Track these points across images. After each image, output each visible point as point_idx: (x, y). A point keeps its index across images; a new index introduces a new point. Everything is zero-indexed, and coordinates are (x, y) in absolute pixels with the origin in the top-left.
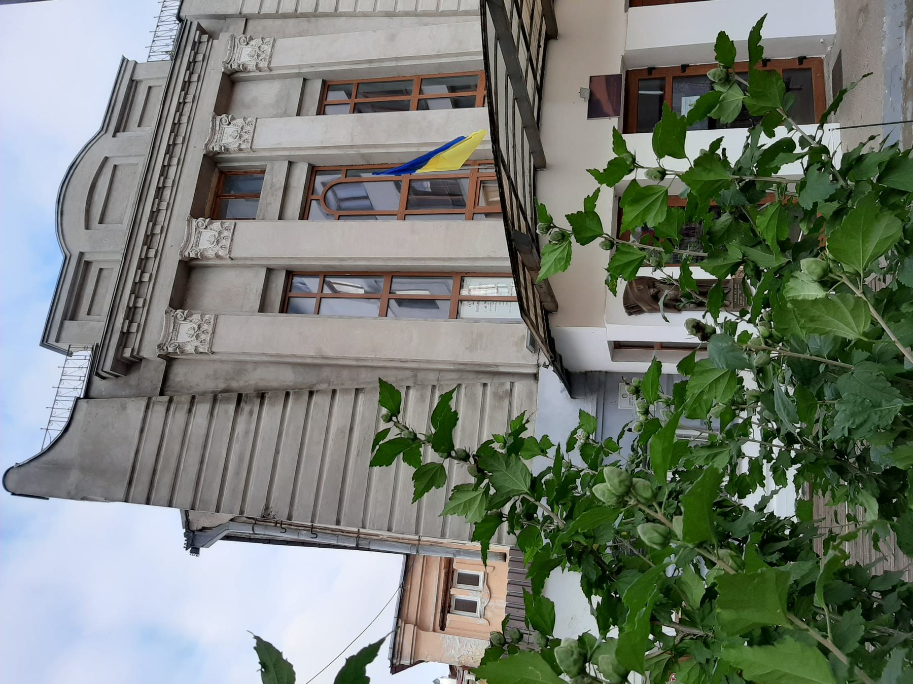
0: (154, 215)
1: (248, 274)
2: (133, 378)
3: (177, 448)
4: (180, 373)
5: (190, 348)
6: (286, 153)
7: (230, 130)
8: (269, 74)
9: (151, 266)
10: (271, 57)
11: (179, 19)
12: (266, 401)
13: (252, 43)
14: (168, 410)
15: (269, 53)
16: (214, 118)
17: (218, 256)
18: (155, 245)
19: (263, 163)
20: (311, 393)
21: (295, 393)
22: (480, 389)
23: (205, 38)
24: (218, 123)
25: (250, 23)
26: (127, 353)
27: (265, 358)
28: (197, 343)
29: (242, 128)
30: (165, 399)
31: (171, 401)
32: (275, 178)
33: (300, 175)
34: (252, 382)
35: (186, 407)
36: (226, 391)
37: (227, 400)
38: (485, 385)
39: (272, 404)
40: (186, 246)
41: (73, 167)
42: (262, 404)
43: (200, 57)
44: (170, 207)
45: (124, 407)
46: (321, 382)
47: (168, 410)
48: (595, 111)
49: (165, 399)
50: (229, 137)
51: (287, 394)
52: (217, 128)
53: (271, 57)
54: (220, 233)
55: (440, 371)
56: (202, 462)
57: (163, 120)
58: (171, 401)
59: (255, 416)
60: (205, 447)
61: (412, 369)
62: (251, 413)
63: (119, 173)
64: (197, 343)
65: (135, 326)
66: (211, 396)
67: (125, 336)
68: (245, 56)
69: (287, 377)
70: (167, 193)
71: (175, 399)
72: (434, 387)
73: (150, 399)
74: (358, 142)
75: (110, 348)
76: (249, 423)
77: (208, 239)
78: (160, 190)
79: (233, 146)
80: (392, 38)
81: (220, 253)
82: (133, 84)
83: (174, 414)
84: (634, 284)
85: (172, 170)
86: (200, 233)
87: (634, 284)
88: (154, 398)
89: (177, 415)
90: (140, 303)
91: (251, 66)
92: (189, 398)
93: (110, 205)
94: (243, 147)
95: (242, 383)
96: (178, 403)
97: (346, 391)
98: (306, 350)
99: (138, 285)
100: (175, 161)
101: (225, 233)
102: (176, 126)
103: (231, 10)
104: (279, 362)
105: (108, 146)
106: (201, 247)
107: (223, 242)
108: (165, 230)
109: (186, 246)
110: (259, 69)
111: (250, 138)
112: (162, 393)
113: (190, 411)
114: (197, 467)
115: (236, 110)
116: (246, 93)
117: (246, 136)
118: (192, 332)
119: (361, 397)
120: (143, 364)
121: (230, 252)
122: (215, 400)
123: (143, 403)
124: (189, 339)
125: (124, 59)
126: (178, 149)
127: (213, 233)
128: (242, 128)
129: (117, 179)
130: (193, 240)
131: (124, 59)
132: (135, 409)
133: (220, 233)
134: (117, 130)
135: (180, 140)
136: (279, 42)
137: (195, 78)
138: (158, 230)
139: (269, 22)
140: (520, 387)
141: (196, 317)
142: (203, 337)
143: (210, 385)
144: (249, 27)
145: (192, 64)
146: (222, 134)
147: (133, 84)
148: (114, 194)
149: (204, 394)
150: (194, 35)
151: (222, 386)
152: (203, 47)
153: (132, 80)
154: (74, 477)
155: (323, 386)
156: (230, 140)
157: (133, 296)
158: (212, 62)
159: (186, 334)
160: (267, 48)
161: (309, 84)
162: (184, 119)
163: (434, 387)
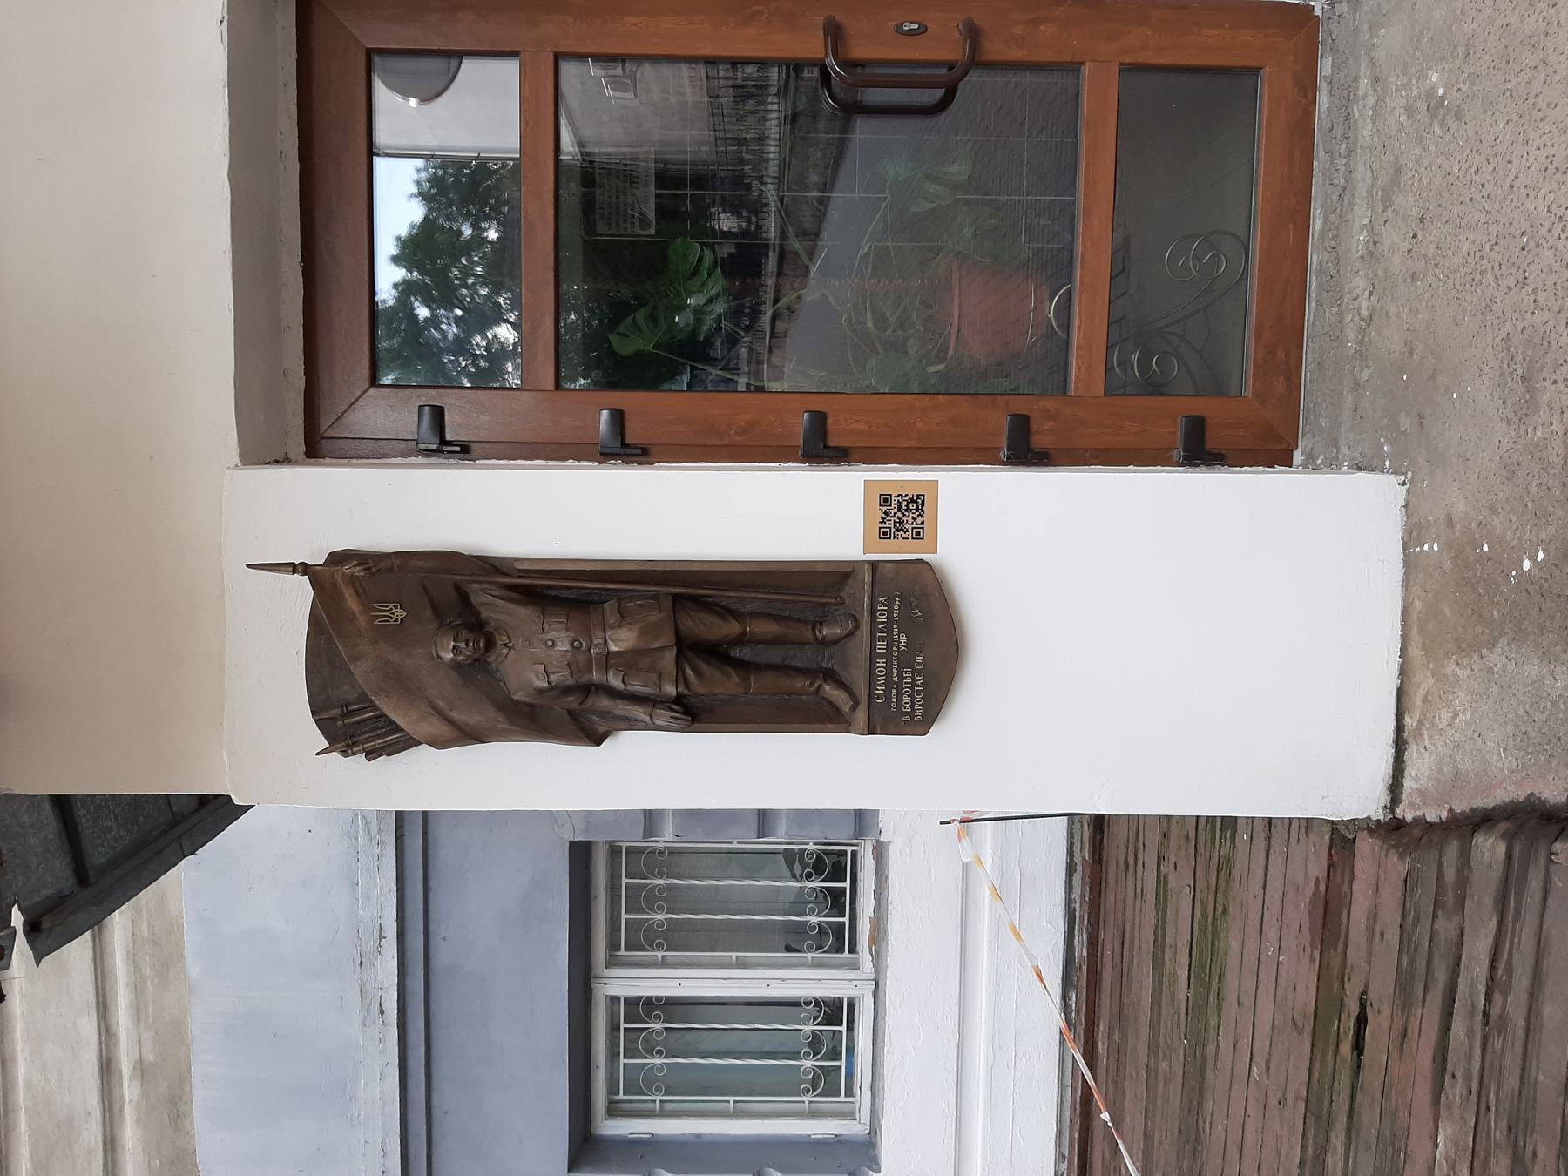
84: (352, 603)
87: (352, 603)
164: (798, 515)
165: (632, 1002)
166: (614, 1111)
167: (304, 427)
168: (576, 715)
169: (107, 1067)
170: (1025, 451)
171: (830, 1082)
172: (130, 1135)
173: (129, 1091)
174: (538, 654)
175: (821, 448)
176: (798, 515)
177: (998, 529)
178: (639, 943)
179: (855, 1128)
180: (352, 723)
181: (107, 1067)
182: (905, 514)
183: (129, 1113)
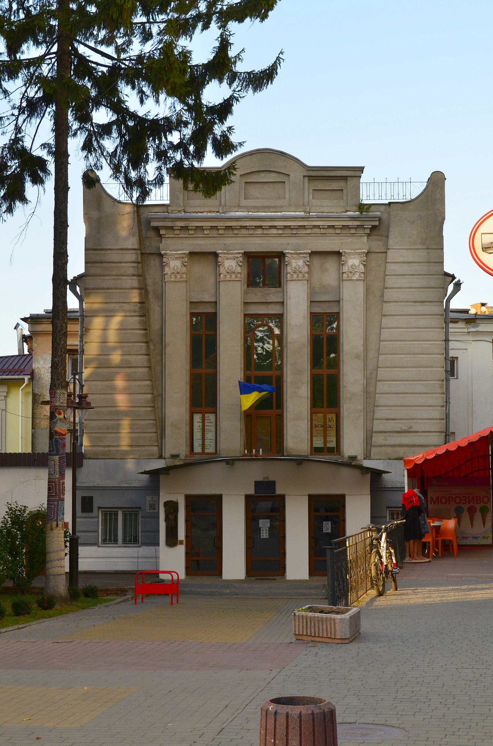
0: (245, 227)
1: (213, 291)
2: (151, 234)
3: (114, 273)
4: (154, 262)
5: (167, 269)
6: (285, 302)
7: (301, 263)
8: (341, 279)
9: (215, 232)
10: (350, 280)
11: (390, 203)
12: (141, 318)
13: (362, 266)
14: (134, 262)
15: (353, 278)
16: (307, 253)
17: (220, 274)
18: (227, 232)
19: (282, 285)
20: (147, 342)
21: (146, 333)
22: (154, 430)
23: (368, 231)
24: (305, 255)
25: (384, 255)
26: (162, 232)
27: (164, 313)
28: (169, 273)
29: (300, 272)
30: (140, 260)
31: (138, 263)
32: (273, 295)
33: (274, 310)
34: (152, 306)
35: (136, 273)
36: (147, 291)
37: (140, 295)
38: (156, 433)
39: (140, 322)
40: (225, 253)
41: (282, 154)
42: (140, 316)
43: (353, 231)
44: (251, 236)
45: (133, 235)
46: (154, 345)
47: (134, 262)
48: (257, 484)
49: (140, 260)
50: (295, 264)
51: (146, 329)
52: (301, 255)
53: (350, 280)
54: (232, 273)
55: (162, 408)
56: (108, 289)
57: (306, 219)
58: (138, 263)
59: (133, 314)
60: (116, 289)
61: (162, 394)
62: (135, 311)
63: (280, 185)
64: (169, 273)
65: (178, 232)
66: (143, 286)
67: (172, 228)
68: (354, 262)
69: (155, 326)
70: (260, 231)
71: (140, 265)
72: (153, 407)
73: (139, 249)
74: (290, 347)
75: (163, 223)
76: (130, 311)
77: (231, 264)
78: (260, 227)
79: (289, 269)
80: (357, 357)
81: (221, 276)
82: (345, 178)
83: (131, 267)
85: (274, 231)
86: (234, 259)
88: (139, 252)
89: (131, 269)
90: (191, 232)
91: (345, 269)
92: (141, 273)
93: (258, 185)
94: (288, 275)
95: (151, 300)
96: (137, 267)
97: (149, 361)
98: (168, 338)
99: (202, 228)
100: (280, 232)
101: (233, 276)
102: (304, 227)
103: (391, 241)
104: (163, 321)
105: (297, 175)
106: (226, 261)
107: (228, 276)
108: (236, 236)
109: (225, 253)
110: (343, 273)
111: (294, 279)
112: (142, 254)
113: (134, 275)
114: (105, 286)
115: (317, 262)
116: (331, 264)
117: (295, 276)
118: (176, 269)
119: (147, 369)
120: (159, 238)
121: (222, 281)
122: (140, 289)
123: (136, 246)
124: (171, 267)
125: (363, 168)
126: (288, 231)
127: (234, 268)
128: (300, 272)
129: (275, 185)
130: (230, 256)
131: (363, 168)
132: (132, 242)
133: (232, 273)
134: (309, 176)
135: (294, 232)
136: (361, 284)
137: (338, 231)
138: (235, 232)
139: (383, 269)
140: (156, 449)
141: (184, 269)
142: (173, 276)
143: (149, 282)
144: (380, 255)
145: (347, 227)
146: (298, 259)
147: (345, 178)
148: (266, 186)
149: (145, 279)
150: (369, 224)
151: (149, 289)
152: (360, 231)
153: (347, 177)
154: (95, 214)
155: (152, 347)
156: (294, 265)
157: (194, 228)
158: (349, 240)
159: (174, 265)
160: (356, 277)
161: (337, 304)
162: (308, 231)
163: (153, 407)
164: (181, 535)
165: (117, 514)
166: (102, 512)
167: (188, 498)
168: (167, 520)
169: (110, 446)
170: (187, 554)
171: (104, 541)
172: (101, 449)
173: (106, 449)
174: (171, 517)
175: (187, 537)
176: (181, 535)
177: (181, 550)
178: (125, 515)
179: (100, 545)
180: (166, 504)
181: (110, 446)
182: (181, 543)
183: (104, 449)
